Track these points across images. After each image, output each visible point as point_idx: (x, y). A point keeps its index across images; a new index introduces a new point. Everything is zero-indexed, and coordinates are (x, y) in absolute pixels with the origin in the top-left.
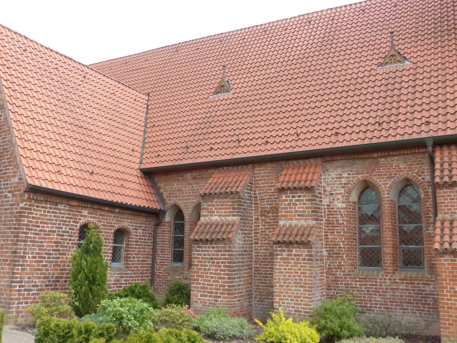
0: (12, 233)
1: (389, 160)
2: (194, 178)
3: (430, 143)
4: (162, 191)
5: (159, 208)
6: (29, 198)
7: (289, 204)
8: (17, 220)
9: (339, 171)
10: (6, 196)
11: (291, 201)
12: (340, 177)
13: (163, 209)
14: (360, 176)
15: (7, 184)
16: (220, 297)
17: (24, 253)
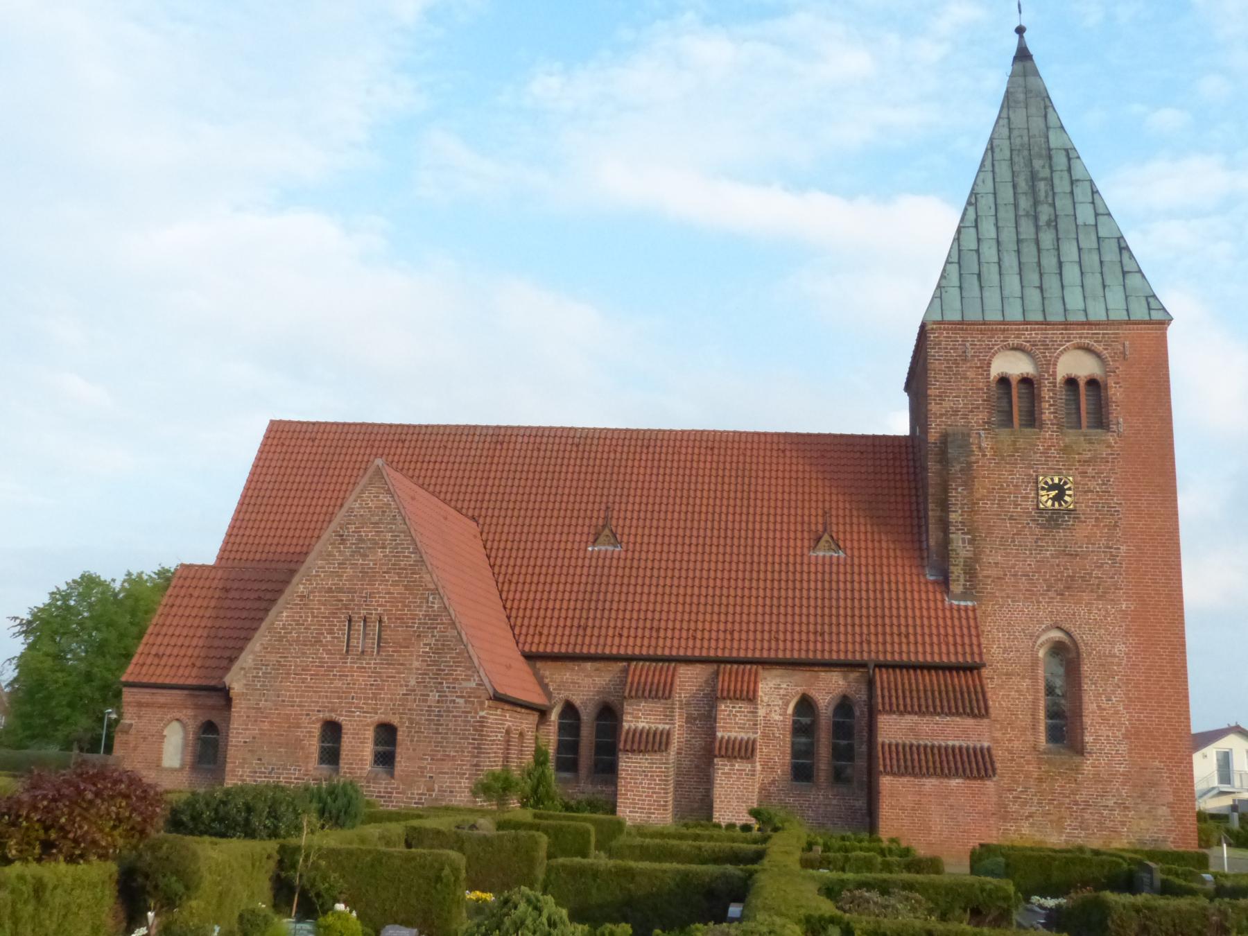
0: (469, 743)
1: (829, 674)
2: (597, 670)
7: (729, 715)
8: (475, 730)
9: (778, 681)
11: (731, 711)
12: (778, 687)
14: (799, 689)
15: (454, 688)
16: (654, 813)
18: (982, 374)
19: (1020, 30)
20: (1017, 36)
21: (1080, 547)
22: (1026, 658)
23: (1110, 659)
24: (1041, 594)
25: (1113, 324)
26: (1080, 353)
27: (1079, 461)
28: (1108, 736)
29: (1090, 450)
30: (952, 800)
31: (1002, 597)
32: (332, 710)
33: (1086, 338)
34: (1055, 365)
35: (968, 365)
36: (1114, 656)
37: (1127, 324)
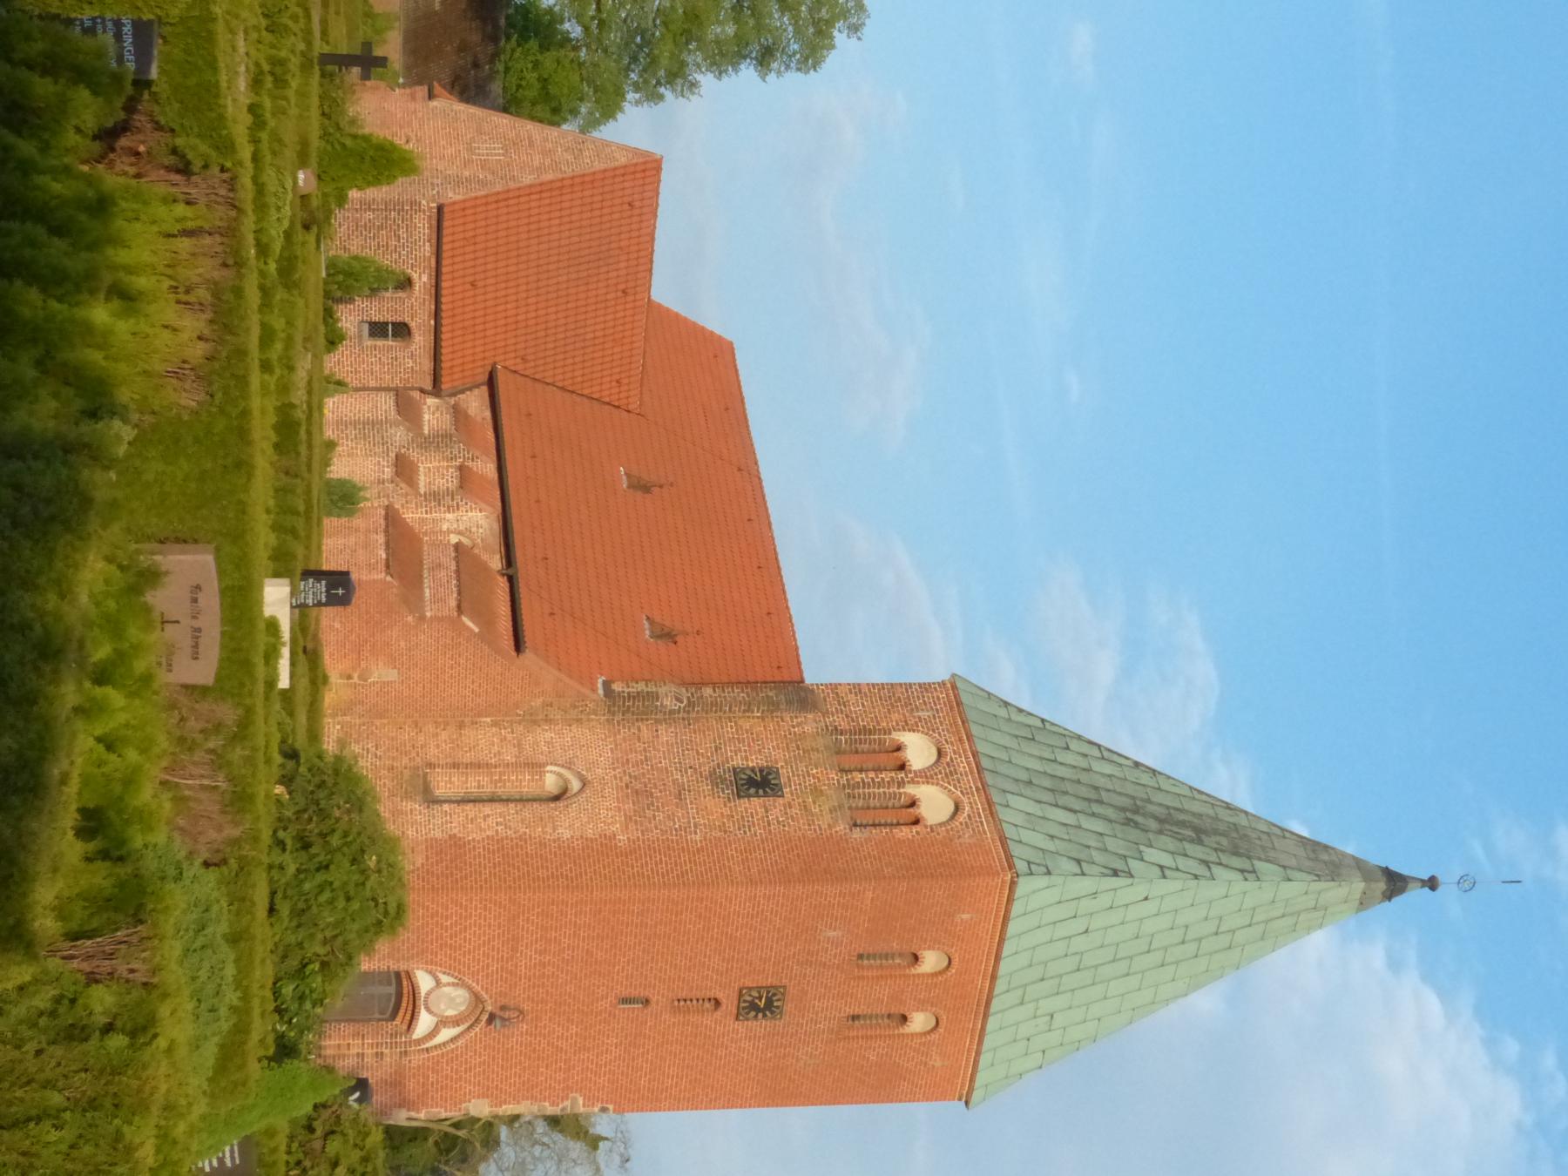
3: (510, 572)
4: (468, 393)
5: (443, 387)
6: (430, 209)
10: (433, 189)
13: (443, 393)
14: (479, 540)
17: (374, 210)
18: (898, 725)
19: (1432, 883)
20: (1426, 877)
21: (691, 803)
22: (543, 759)
23: (550, 825)
24: (625, 772)
25: (996, 826)
26: (952, 808)
27: (804, 802)
28: (451, 823)
29: (821, 811)
30: (360, 551)
31: (615, 741)
32: (417, 140)
33: (972, 807)
34: (928, 783)
35: (907, 714)
36: (554, 829)
37: (1000, 838)
